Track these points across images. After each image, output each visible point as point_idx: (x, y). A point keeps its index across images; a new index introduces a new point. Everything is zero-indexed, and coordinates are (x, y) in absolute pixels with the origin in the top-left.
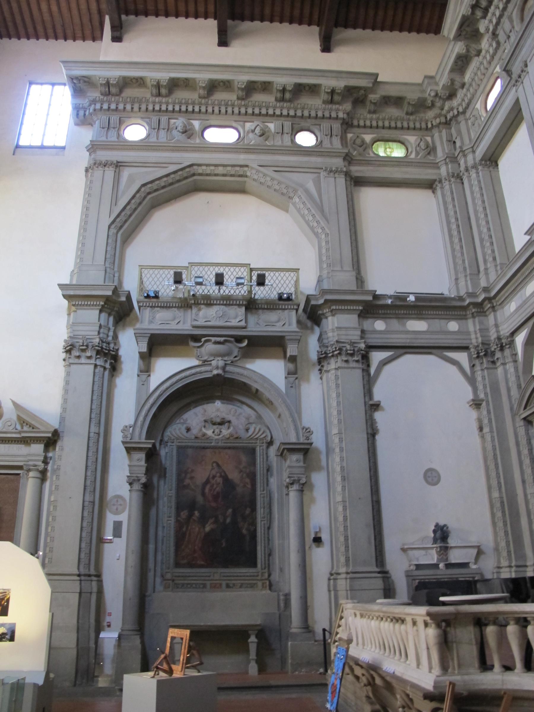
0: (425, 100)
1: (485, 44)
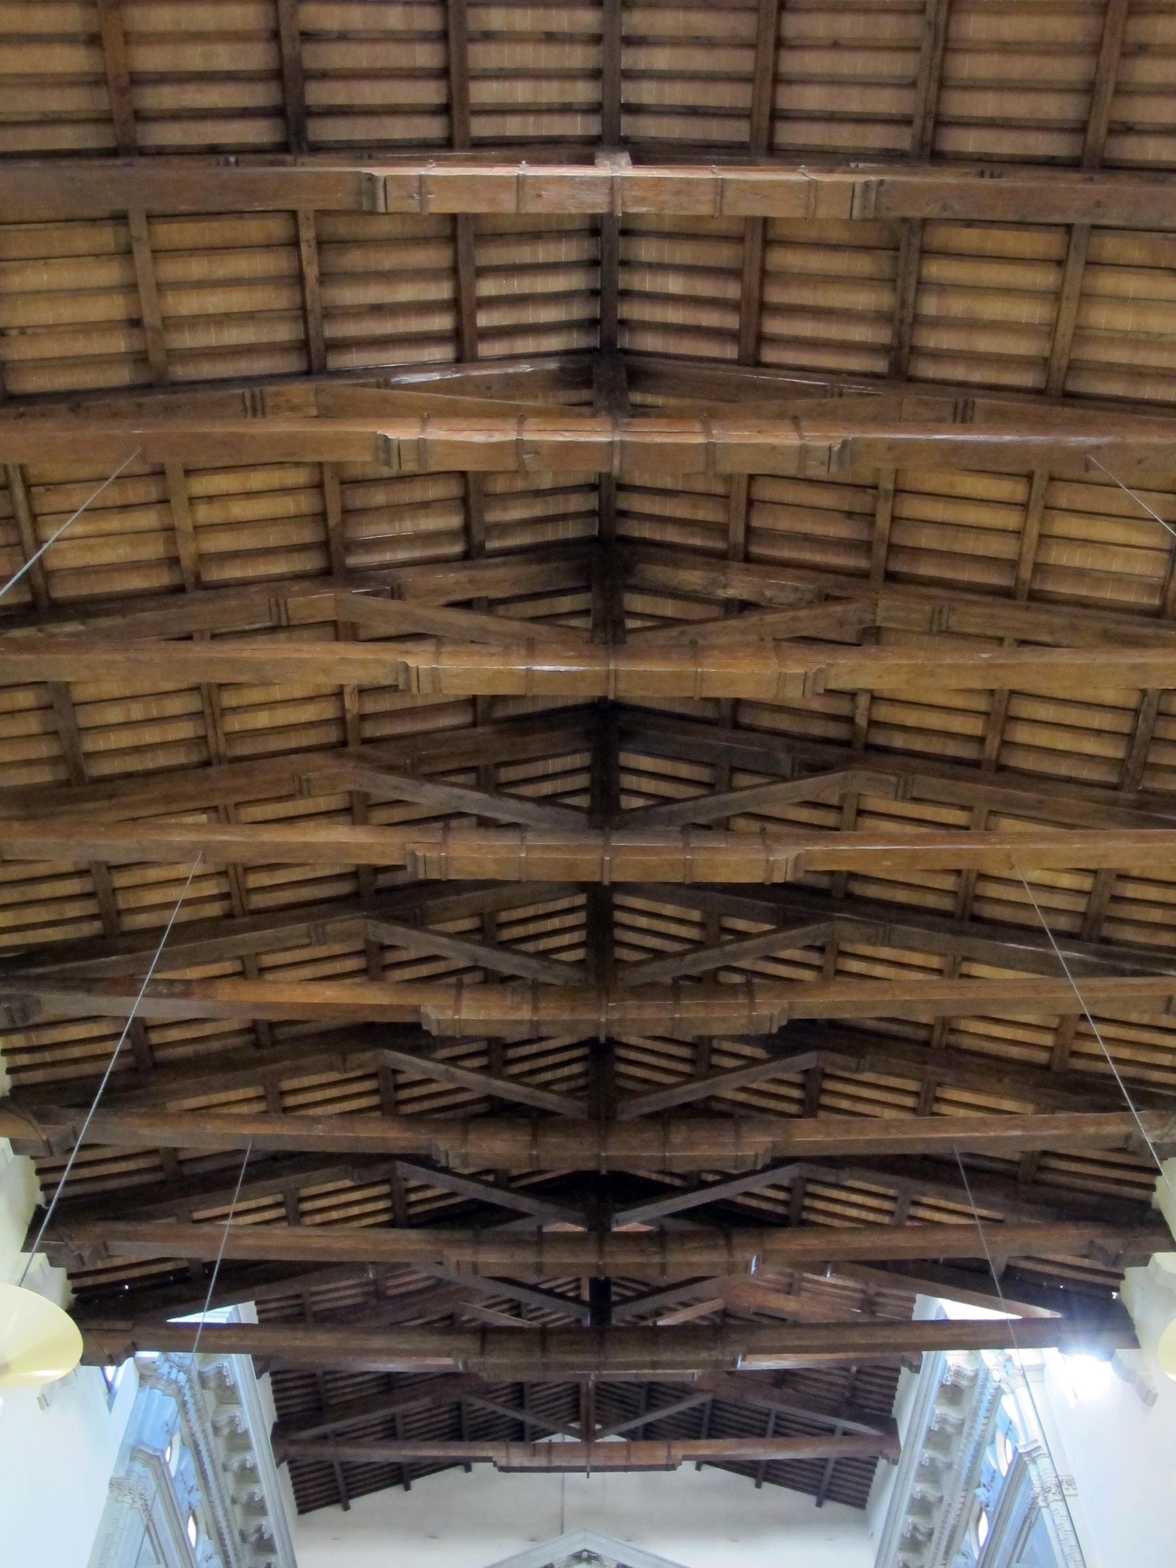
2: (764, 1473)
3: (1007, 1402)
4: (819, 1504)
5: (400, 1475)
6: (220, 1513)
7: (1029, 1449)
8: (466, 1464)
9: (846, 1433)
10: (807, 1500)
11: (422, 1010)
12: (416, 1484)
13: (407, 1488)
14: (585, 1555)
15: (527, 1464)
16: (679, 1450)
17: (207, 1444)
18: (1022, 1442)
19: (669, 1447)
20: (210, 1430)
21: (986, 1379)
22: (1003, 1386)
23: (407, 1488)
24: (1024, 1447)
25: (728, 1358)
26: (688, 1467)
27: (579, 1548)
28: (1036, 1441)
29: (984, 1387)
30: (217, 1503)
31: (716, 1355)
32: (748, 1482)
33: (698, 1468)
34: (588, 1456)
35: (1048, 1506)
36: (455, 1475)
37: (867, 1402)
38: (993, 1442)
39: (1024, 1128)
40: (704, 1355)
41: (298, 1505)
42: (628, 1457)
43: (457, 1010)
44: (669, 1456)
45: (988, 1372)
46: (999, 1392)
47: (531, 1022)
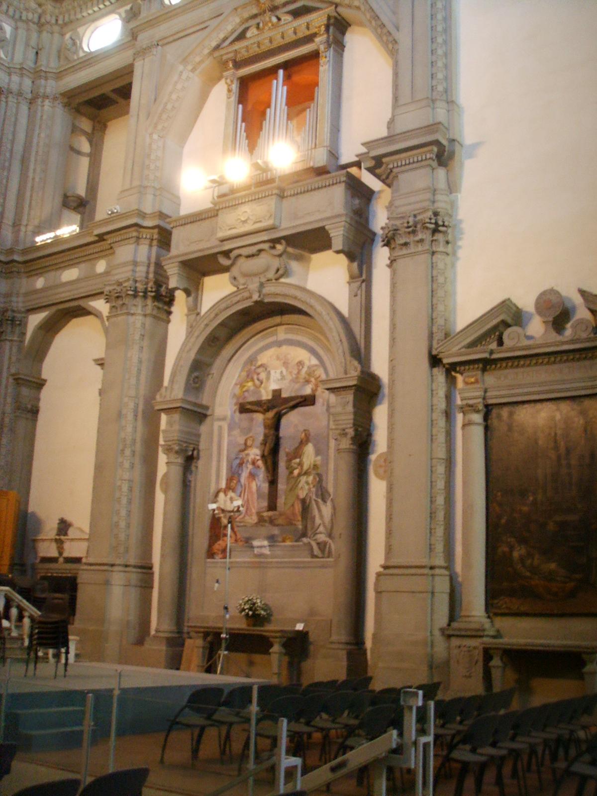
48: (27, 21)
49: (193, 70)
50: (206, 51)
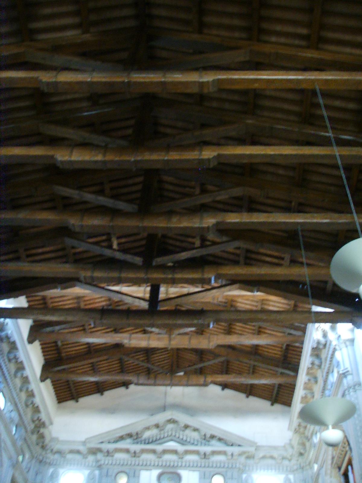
0: (46, 446)
1: (91, 458)
2: (250, 391)
3: (338, 355)
4: (272, 405)
5: (99, 388)
6: (15, 396)
7: (344, 371)
8: (126, 384)
9: (282, 374)
10: (267, 404)
11: (55, 157)
12: (107, 393)
13: (102, 394)
14: (172, 420)
15: (146, 382)
16: (209, 379)
17: (6, 365)
18: (342, 368)
19: (205, 378)
20: (6, 360)
21: (330, 345)
22: (337, 347)
23: (102, 394)
24: (343, 371)
25: (206, 323)
26: (217, 389)
27: (169, 418)
28: (347, 368)
29: (329, 348)
30: (13, 390)
31: (200, 322)
32: (242, 396)
33: (223, 389)
34: (171, 380)
35: (349, 394)
36: (121, 390)
37: (289, 359)
38: (333, 372)
39: (331, 219)
40: (195, 322)
41: (58, 399)
42: (188, 381)
43: (71, 156)
44: (205, 381)
45: (331, 342)
46: (335, 350)
47: (101, 161)
48: (297, 470)
49: (331, 477)
50: (329, 467)
